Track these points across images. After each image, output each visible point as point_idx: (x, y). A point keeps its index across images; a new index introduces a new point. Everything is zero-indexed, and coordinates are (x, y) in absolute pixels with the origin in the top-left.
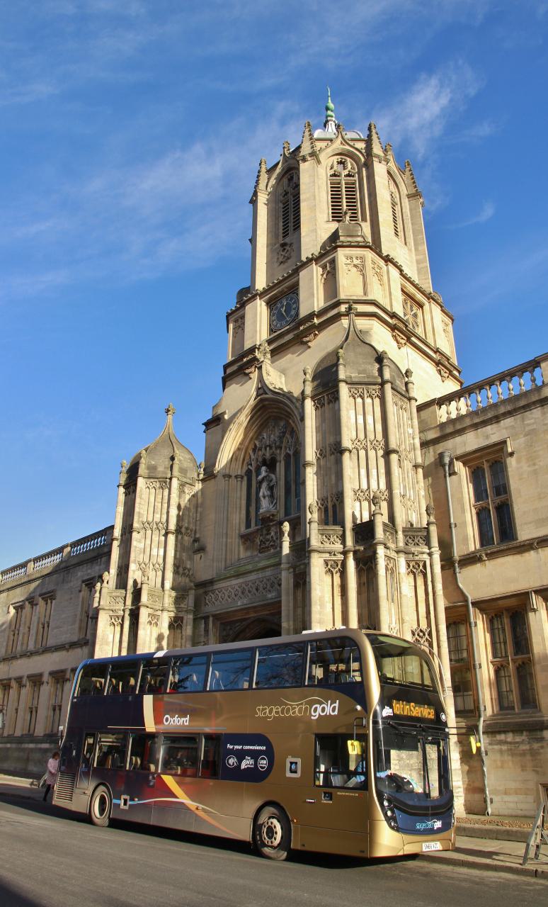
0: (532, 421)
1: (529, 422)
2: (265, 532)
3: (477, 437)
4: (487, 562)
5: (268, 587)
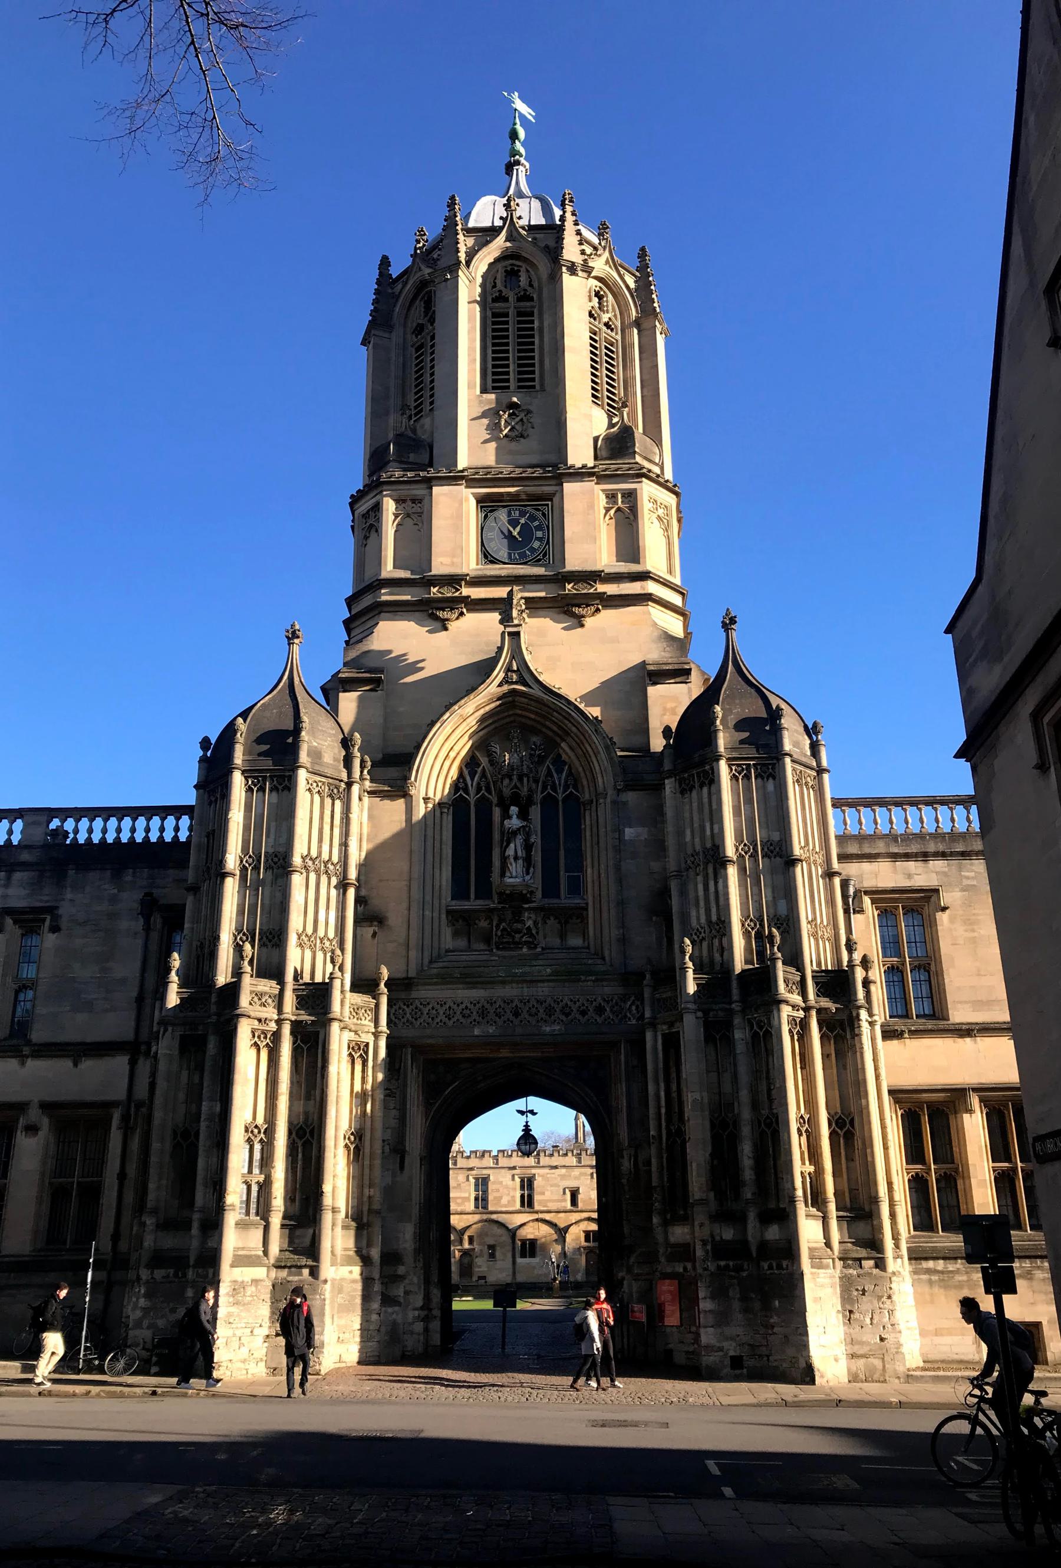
0: (972, 874)
1: (967, 874)
2: (509, 915)
3: (895, 871)
4: (907, 1041)
5: (542, 1014)
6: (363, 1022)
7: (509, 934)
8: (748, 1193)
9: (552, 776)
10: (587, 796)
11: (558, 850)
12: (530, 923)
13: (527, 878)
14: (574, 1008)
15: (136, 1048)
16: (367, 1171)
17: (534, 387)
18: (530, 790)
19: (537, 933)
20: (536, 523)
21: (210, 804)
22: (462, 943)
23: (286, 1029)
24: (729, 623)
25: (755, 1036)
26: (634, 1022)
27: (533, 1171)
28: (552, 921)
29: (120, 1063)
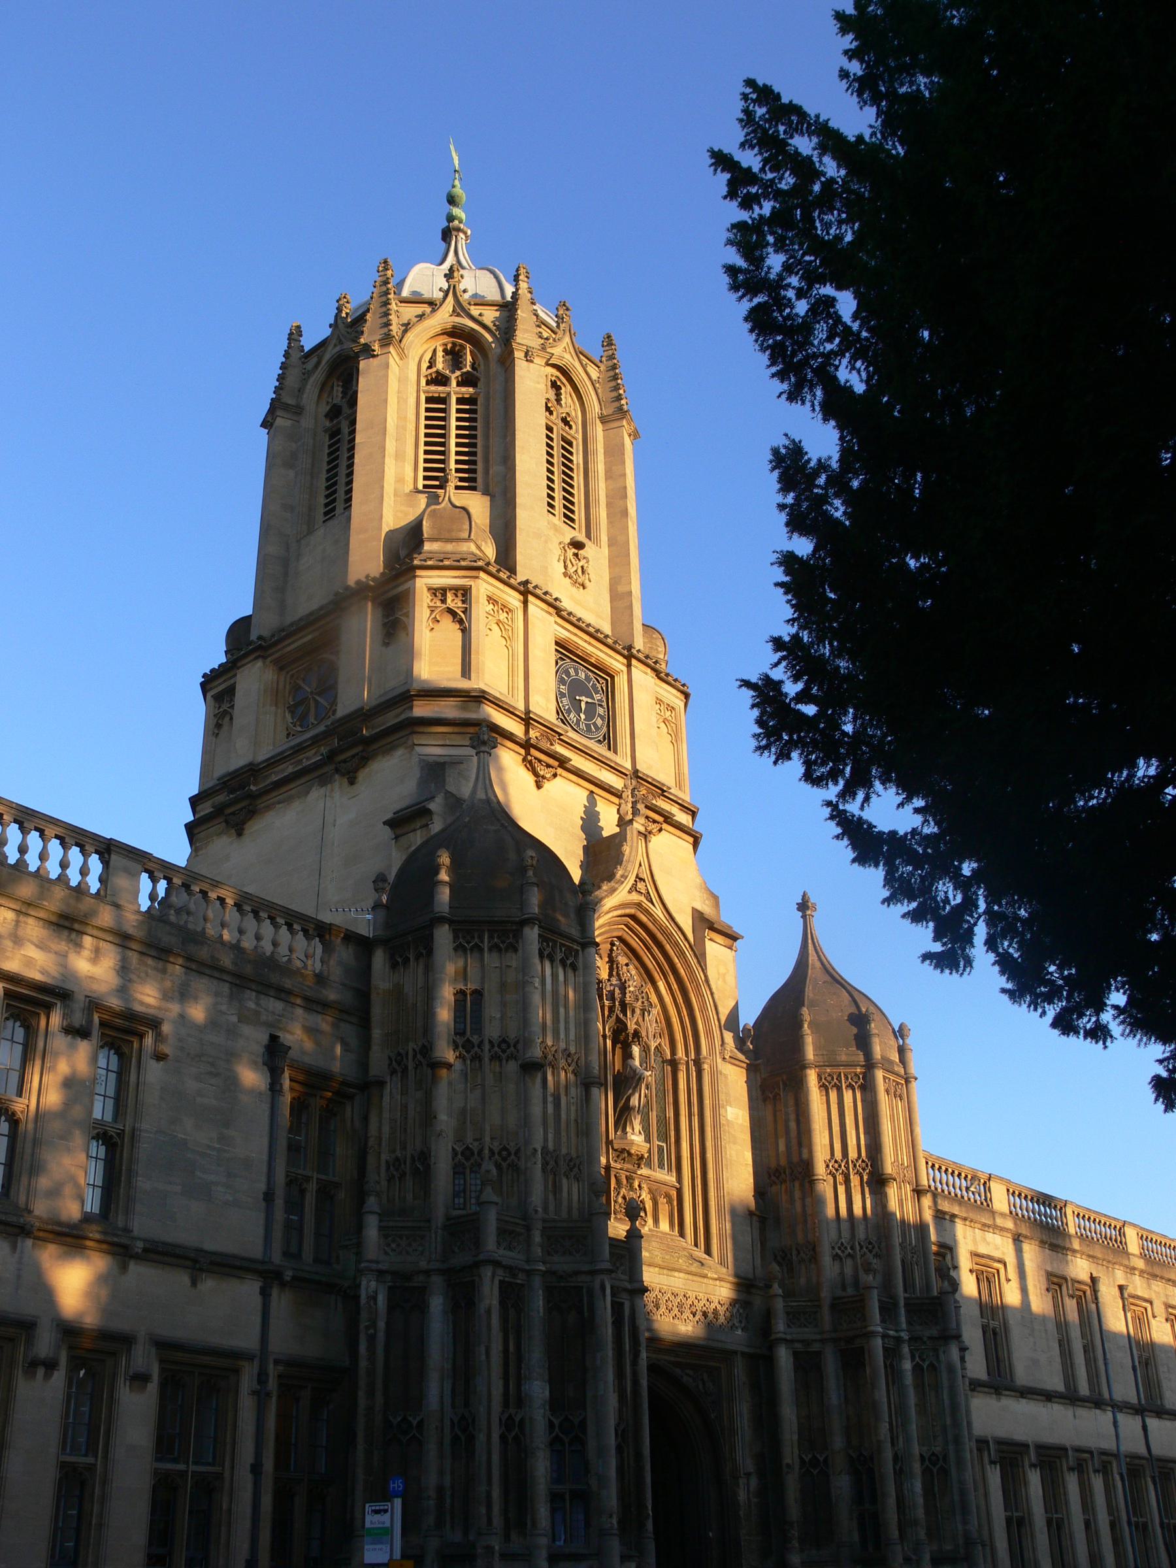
25: (917, 1369)
26: (739, 1332)
29: (249, 1290)
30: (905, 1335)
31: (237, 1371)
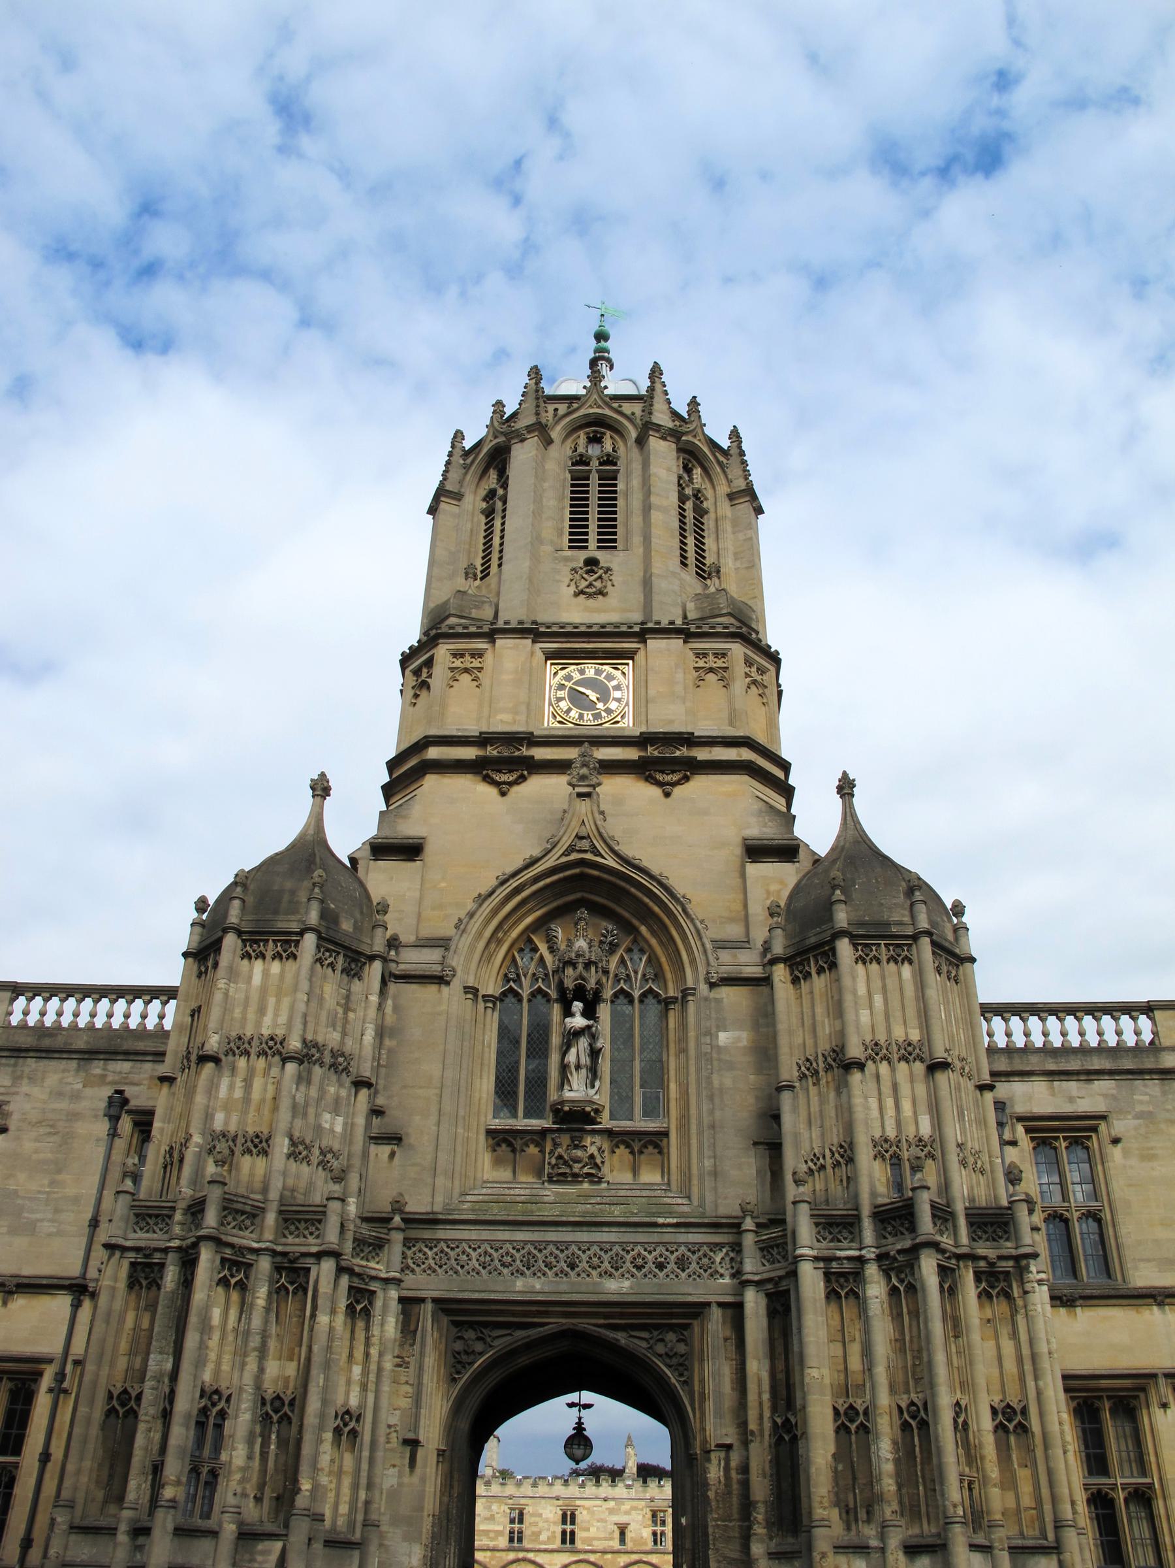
0: (1146, 1098)
1: (1141, 1097)
2: (565, 1139)
3: (1053, 1095)
5: (606, 1265)
6: (372, 1264)
7: (566, 1163)
8: (889, 1510)
9: (627, 968)
10: (671, 993)
11: (633, 1060)
12: (593, 1150)
13: (592, 1092)
14: (650, 1257)
15: (79, 1289)
16: (365, 1466)
17: (615, 547)
18: (598, 982)
19: (603, 1163)
20: (614, 683)
21: (199, 976)
22: (505, 1174)
23: (264, 1264)
24: (846, 788)
25: (893, 1292)
26: (727, 1280)
27: (578, 1502)
28: (622, 1150)
29: (61, 1303)
30: (869, 1253)
31: (40, 1374)
